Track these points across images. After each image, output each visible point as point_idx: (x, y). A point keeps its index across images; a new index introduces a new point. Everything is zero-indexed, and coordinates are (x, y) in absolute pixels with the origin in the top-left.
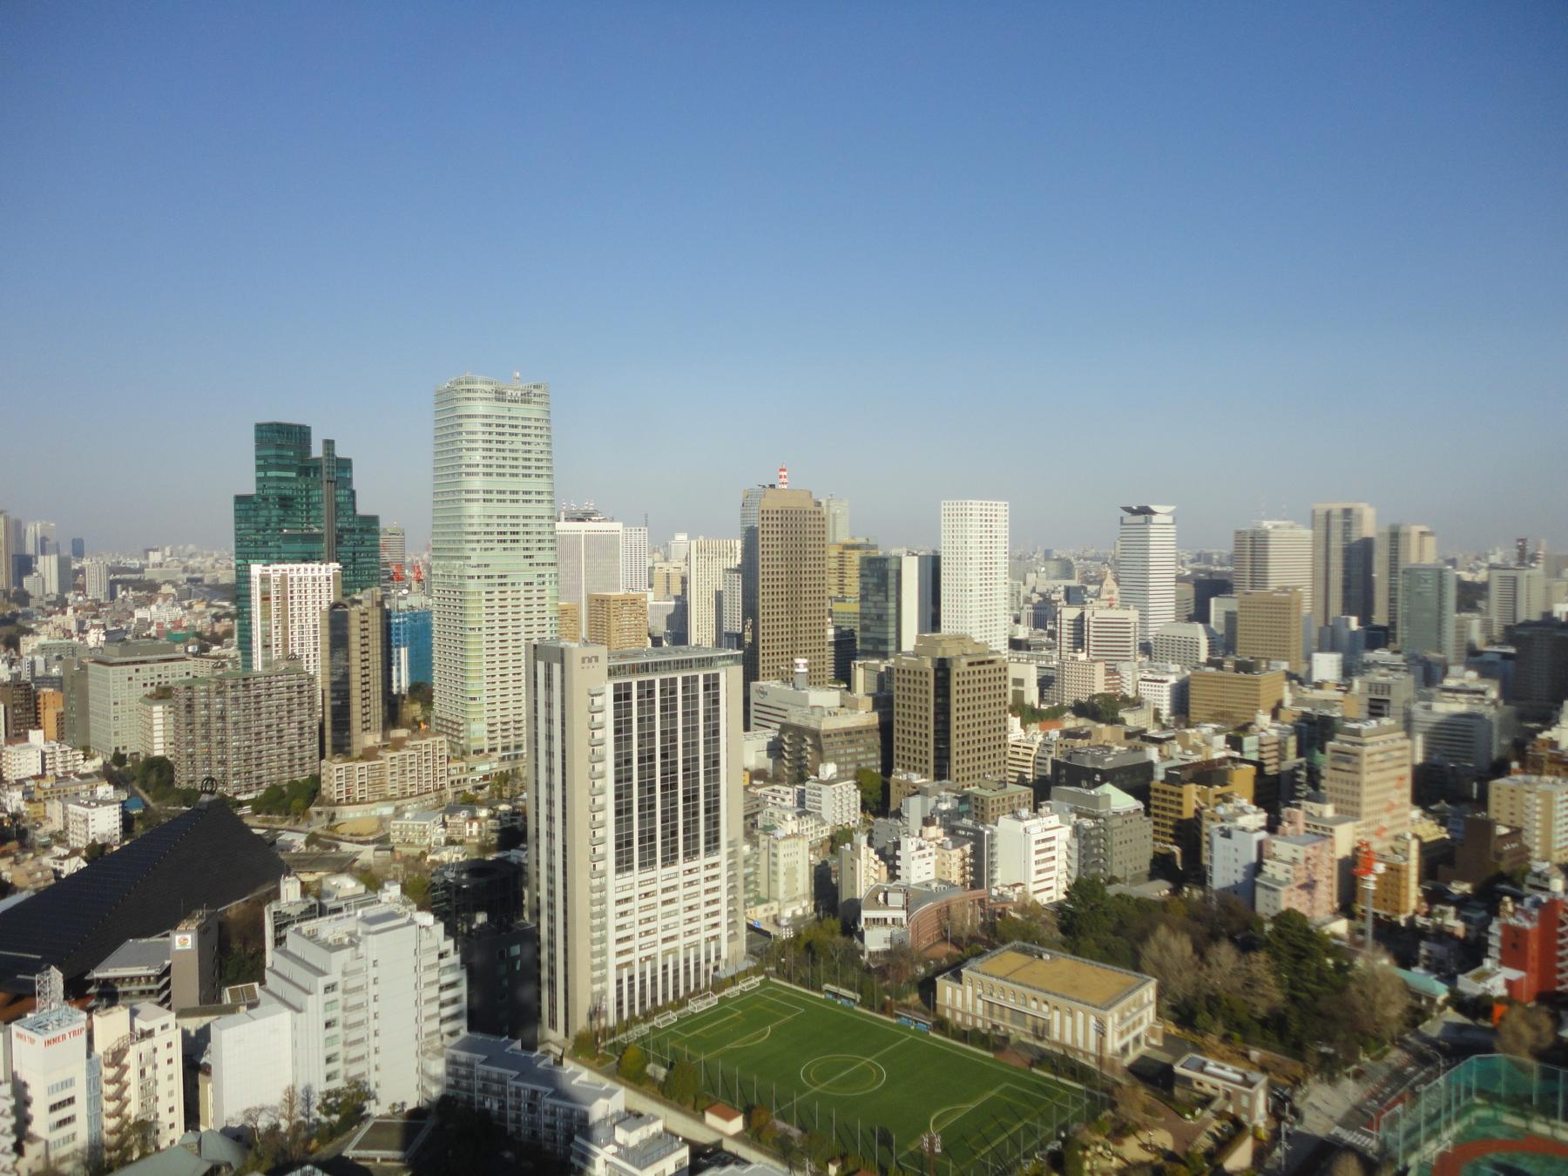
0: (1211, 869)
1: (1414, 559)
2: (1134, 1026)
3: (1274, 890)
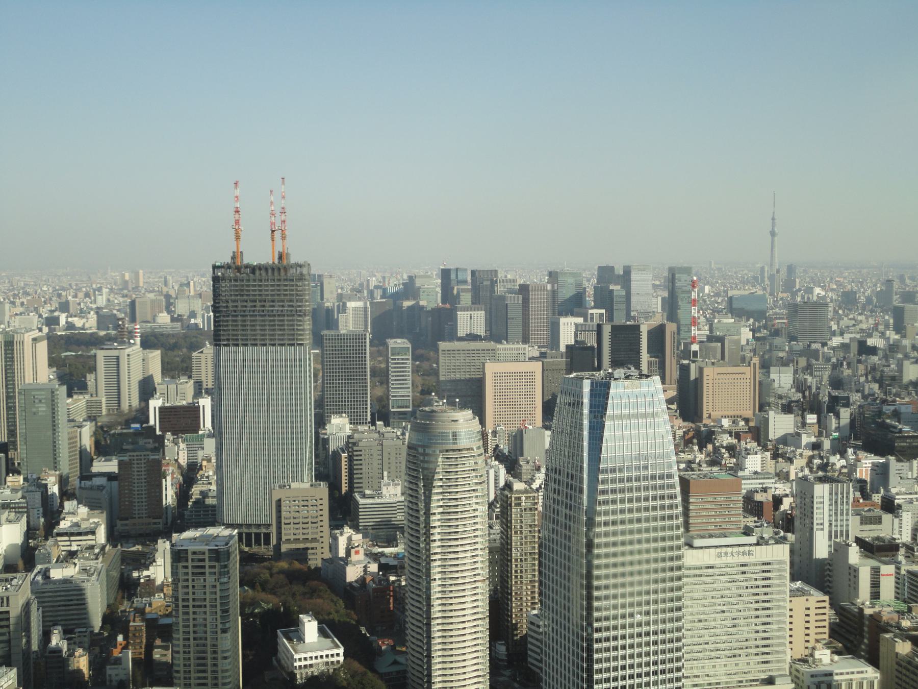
1: (29, 379)
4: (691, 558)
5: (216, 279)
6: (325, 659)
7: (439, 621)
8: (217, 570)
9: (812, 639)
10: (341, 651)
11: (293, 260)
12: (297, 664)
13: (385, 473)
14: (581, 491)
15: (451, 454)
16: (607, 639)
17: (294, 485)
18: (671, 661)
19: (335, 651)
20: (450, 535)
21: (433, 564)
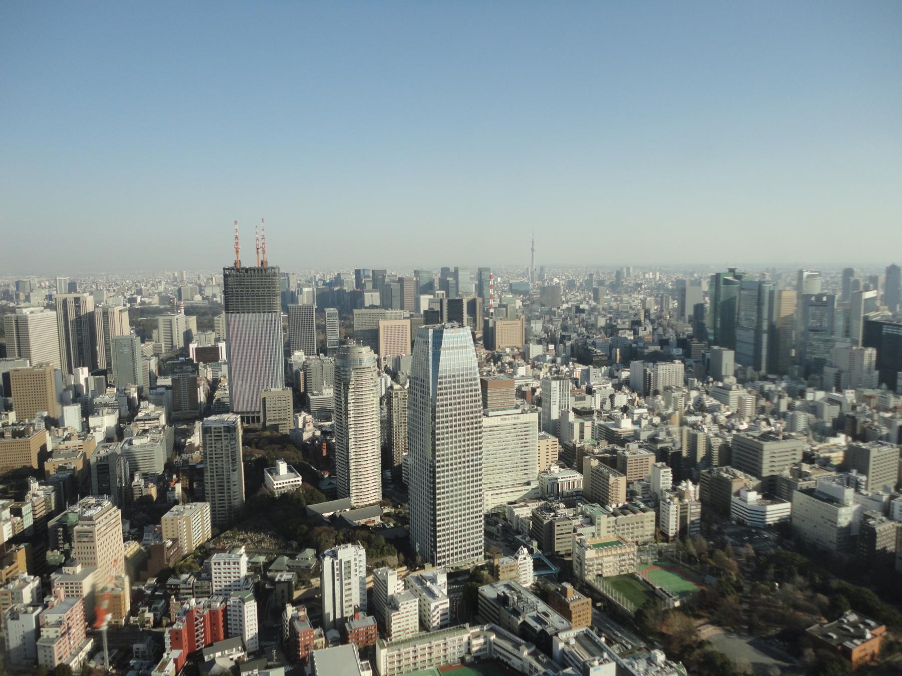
0: (8, 640)
1: (118, 333)
3: (49, 647)
4: (486, 422)
5: (225, 276)
6: (291, 483)
7: (354, 460)
8: (228, 437)
9: (550, 461)
10: (300, 479)
11: (269, 266)
12: (275, 487)
14: (429, 390)
15: (359, 371)
16: (443, 466)
17: (273, 390)
18: (476, 476)
19: (297, 479)
20: (359, 415)
21: (350, 430)
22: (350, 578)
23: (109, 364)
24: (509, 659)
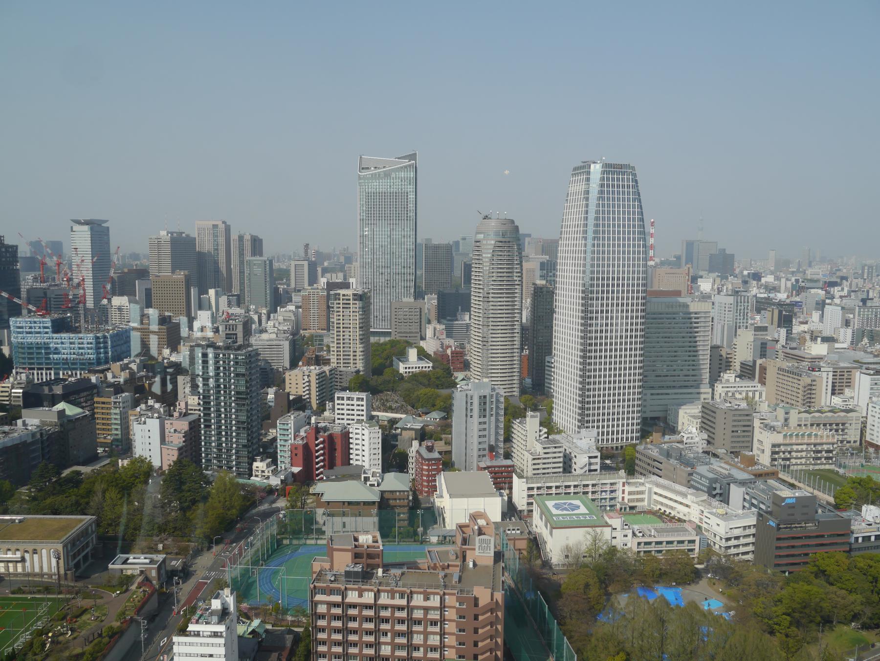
2: (83, 549)
8: (357, 306)
10: (431, 365)
13: (460, 308)
22: (485, 416)
23: (242, 290)
24: (672, 508)
